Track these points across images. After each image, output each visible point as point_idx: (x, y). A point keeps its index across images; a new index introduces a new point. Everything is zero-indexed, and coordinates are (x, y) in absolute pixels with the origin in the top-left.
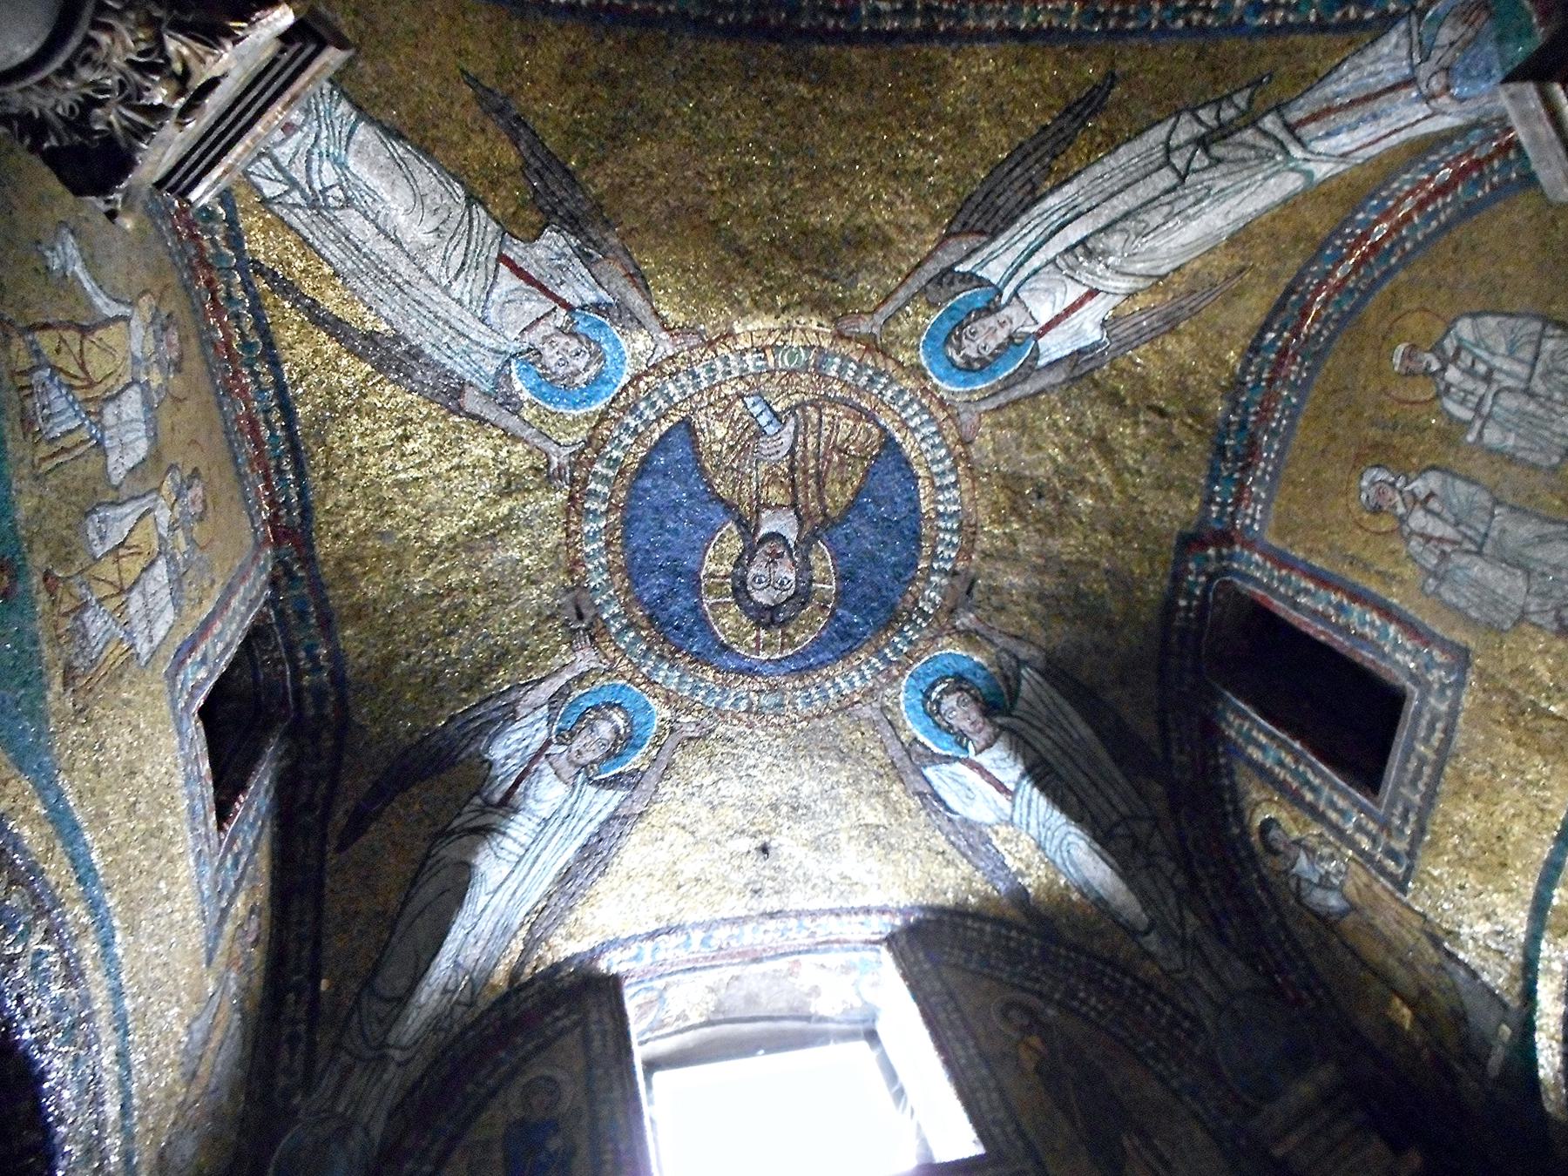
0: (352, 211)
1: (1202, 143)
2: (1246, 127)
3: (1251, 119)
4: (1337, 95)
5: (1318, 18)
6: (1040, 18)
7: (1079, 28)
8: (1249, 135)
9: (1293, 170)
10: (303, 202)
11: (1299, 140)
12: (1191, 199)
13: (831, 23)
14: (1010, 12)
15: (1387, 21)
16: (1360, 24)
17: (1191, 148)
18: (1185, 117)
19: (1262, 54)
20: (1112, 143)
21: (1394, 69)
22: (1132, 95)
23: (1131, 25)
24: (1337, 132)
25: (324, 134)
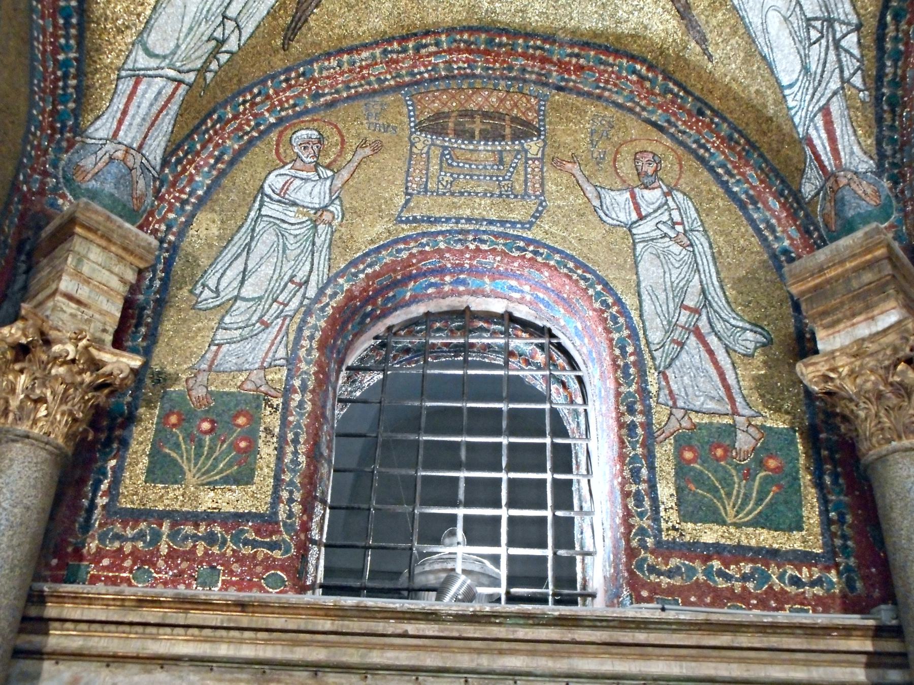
0: (809, 15)
1: (221, 42)
2: (202, 67)
3: (202, 71)
4: (167, 114)
5: (193, 139)
6: (336, 63)
7: (312, 65)
8: (198, 64)
9: (165, 57)
10: (837, 25)
11: (174, 80)
12: (214, 9)
13: (466, 36)
14: (355, 62)
15: (165, 162)
16: (173, 152)
17: (226, 35)
18: (235, 48)
19: (209, 102)
20: (272, 13)
21: (151, 145)
22: (270, 44)
23: (282, 77)
24: (156, 99)
25: (808, 97)
